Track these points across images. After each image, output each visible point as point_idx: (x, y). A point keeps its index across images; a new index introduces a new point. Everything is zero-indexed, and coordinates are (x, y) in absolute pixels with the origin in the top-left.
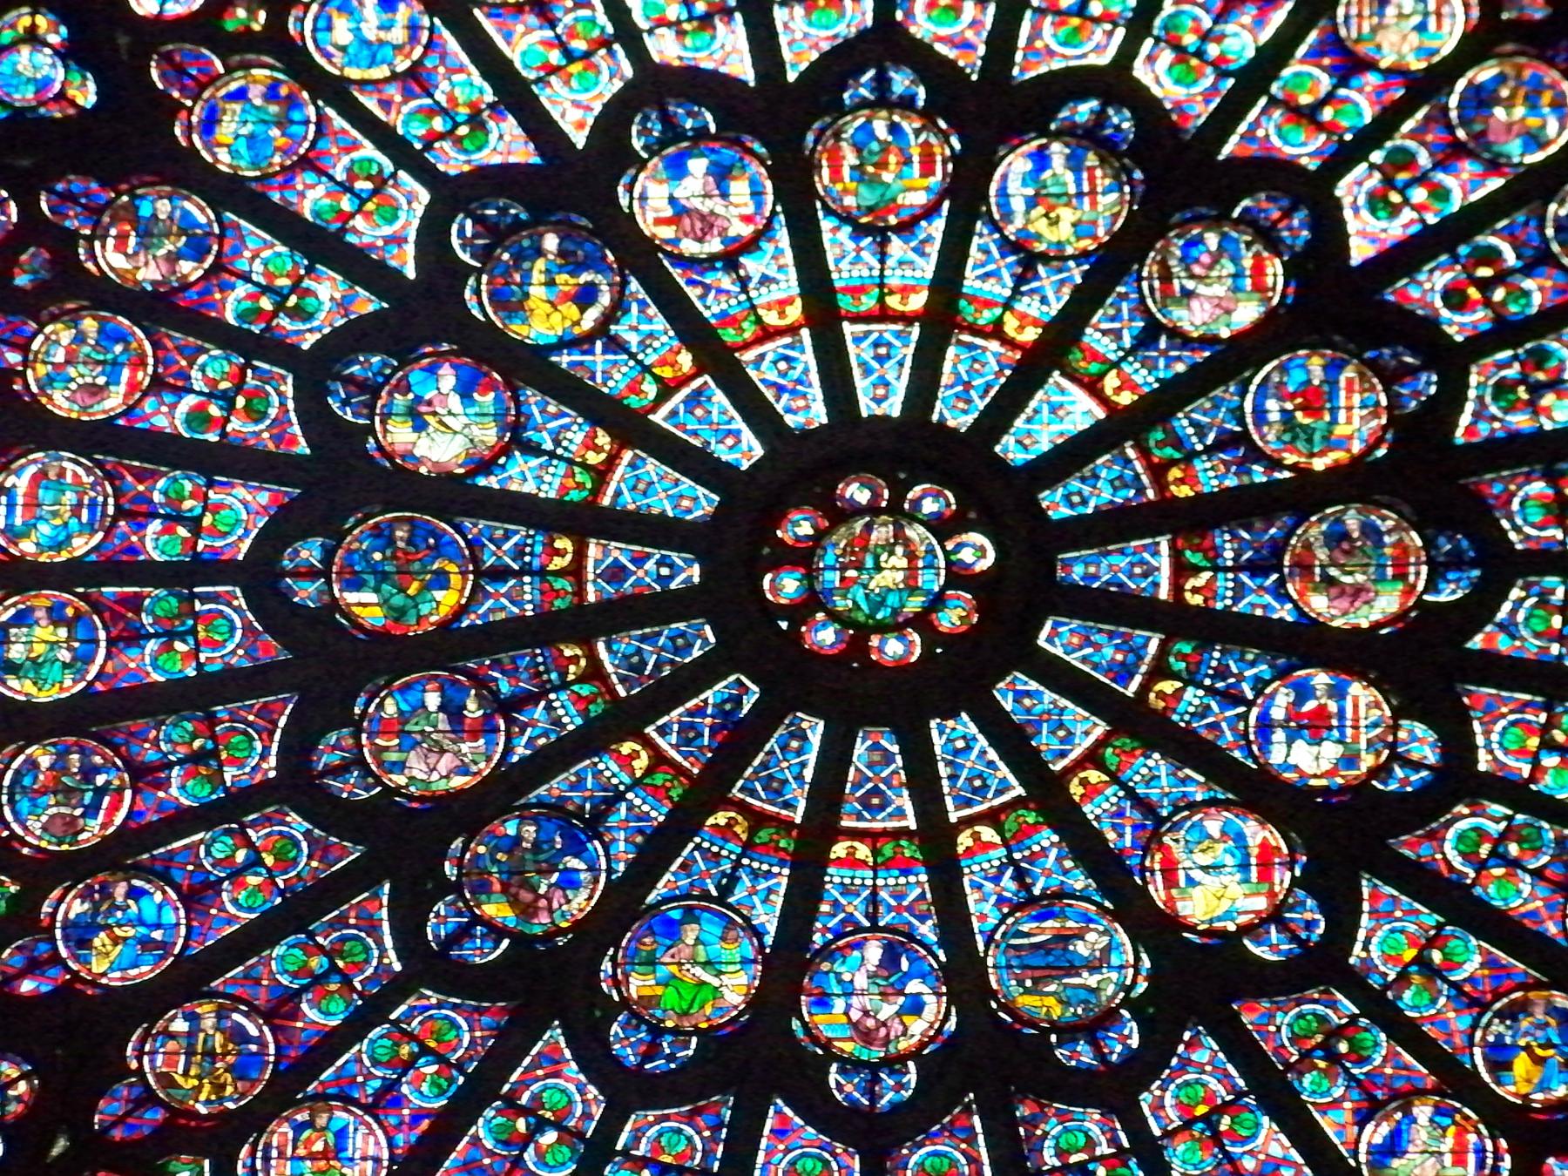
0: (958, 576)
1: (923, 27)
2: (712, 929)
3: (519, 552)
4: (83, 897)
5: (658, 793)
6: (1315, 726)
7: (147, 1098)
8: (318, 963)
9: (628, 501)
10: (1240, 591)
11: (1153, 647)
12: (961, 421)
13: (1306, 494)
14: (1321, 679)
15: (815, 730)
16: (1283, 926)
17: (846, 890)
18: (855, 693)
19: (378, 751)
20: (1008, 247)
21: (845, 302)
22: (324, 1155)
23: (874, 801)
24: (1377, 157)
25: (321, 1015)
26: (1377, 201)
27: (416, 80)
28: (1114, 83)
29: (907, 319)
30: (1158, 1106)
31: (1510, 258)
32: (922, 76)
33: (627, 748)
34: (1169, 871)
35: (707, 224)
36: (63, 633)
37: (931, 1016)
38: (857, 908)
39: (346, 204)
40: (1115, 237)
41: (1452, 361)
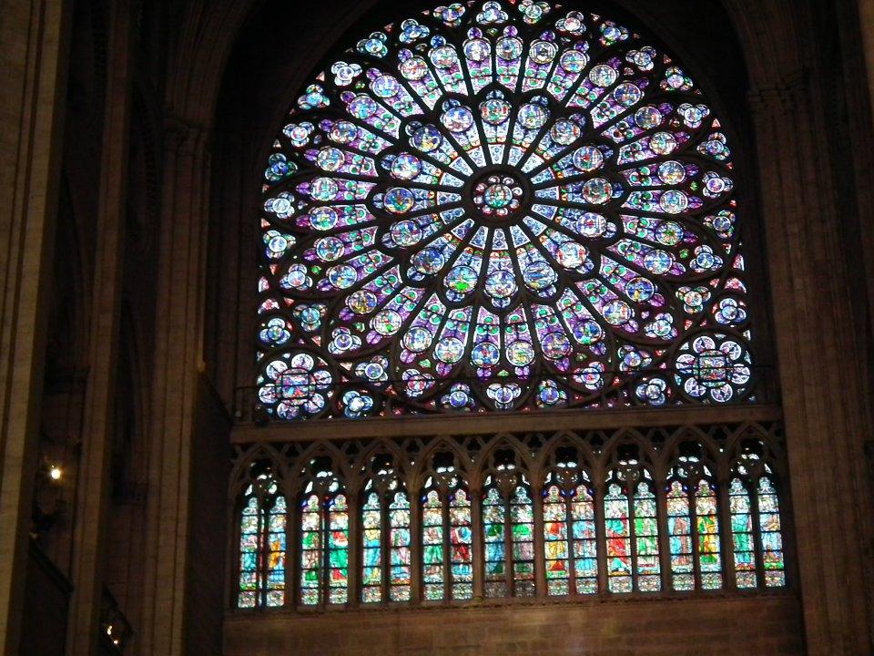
0: (515, 197)
1: (502, 81)
2: (465, 272)
3: (423, 195)
4: (335, 270)
6: (590, 225)
7: (351, 311)
8: (385, 282)
9: (445, 184)
11: (555, 210)
12: (514, 164)
13: (586, 177)
14: (591, 215)
15: (486, 229)
16: (585, 266)
17: (494, 263)
18: (494, 222)
19: (396, 238)
20: (523, 127)
21: (489, 141)
24: (599, 105)
25: (386, 293)
26: (599, 115)
27: (396, 97)
28: (543, 92)
29: (501, 143)
30: (560, 305)
31: (627, 125)
32: (503, 93)
33: (447, 235)
35: (459, 125)
36: (328, 216)
37: (512, 288)
38: (496, 266)
39: (384, 124)
40: (545, 125)
41: (616, 147)
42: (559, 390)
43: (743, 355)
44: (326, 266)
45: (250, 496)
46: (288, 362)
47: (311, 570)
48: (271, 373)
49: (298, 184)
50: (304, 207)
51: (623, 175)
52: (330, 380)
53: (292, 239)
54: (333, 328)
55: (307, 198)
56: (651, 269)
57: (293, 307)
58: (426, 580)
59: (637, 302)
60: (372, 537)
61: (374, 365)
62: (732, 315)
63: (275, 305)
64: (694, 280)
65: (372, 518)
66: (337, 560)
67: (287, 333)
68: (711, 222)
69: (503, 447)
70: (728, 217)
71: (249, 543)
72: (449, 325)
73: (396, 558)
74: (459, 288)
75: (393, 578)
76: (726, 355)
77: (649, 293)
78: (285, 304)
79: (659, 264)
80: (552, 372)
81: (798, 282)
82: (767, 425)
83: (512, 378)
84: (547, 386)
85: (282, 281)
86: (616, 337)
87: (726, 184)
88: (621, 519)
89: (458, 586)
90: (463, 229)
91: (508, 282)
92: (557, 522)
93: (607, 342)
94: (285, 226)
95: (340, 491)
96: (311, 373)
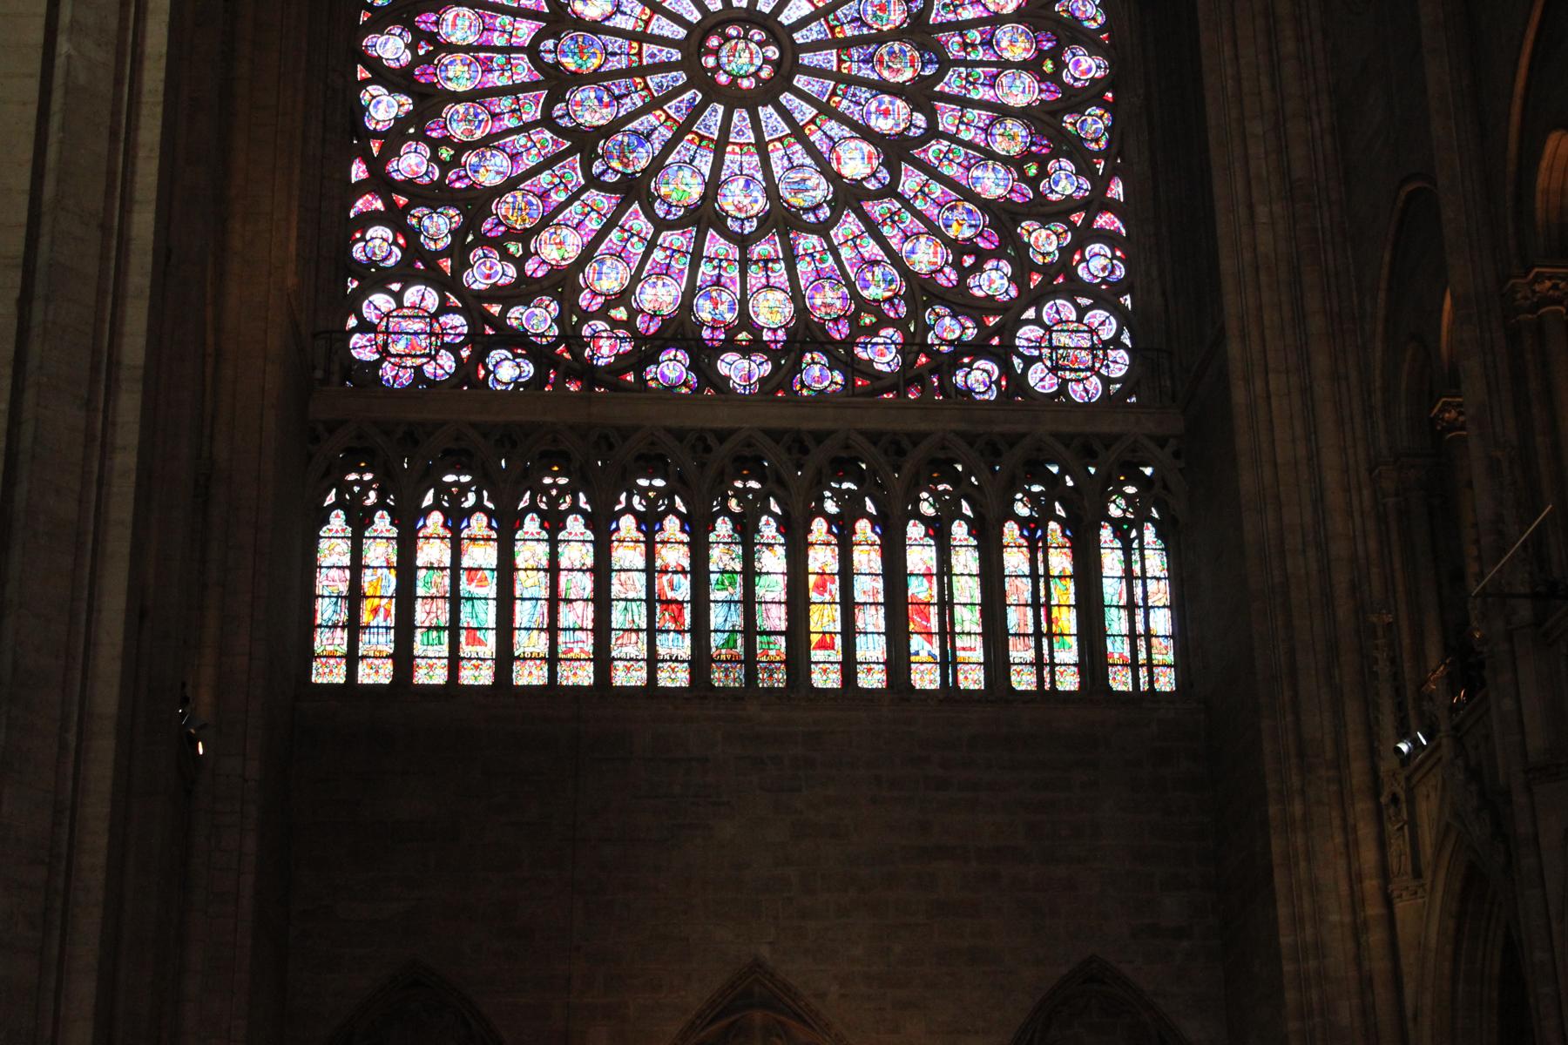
0: (766, 60)
2: (687, 172)
5: (669, 128)
6: (886, 113)
8: (557, 181)
9: (656, 32)
10: (860, 69)
12: (767, 10)
13: (881, 38)
14: (887, 98)
15: (720, 109)
18: (733, 97)
22: (561, 243)
23: (740, 133)
25: (559, 197)
33: (658, 113)
34: (838, 159)
37: (760, 204)
38: (736, 168)
42: (831, 369)
43: (1119, 333)
44: (462, 147)
45: (333, 507)
46: (398, 297)
47: (429, 628)
48: (369, 314)
49: (419, 15)
50: (428, 52)
51: (939, 40)
52: (465, 330)
53: (407, 103)
54: (472, 246)
55: (432, 38)
56: (979, 189)
57: (406, 209)
58: (614, 654)
59: (956, 240)
60: (530, 584)
61: (537, 311)
62: (1104, 269)
63: (379, 205)
64: (1046, 212)
65: (530, 551)
66: (475, 616)
67: (396, 250)
68: (1074, 124)
69: (747, 452)
70: (1101, 117)
71: (331, 581)
72: (658, 255)
73: (567, 616)
74: (675, 197)
75: (561, 648)
76: (1092, 331)
77: (976, 226)
78: (395, 203)
79: (992, 183)
80: (822, 339)
81: (1262, 212)
82: (1161, 442)
83: (756, 346)
84: (813, 362)
85: (390, 168)
86: (921, 291)
87: (1098, 67)
88: (924, 575)
89: (665, 665)
90: (683, 106)
91: (755, 194)
92: (823, 574)
93: (909, 298)
94: (396, 80)
95: (479, 507)
96: (434, 317)
